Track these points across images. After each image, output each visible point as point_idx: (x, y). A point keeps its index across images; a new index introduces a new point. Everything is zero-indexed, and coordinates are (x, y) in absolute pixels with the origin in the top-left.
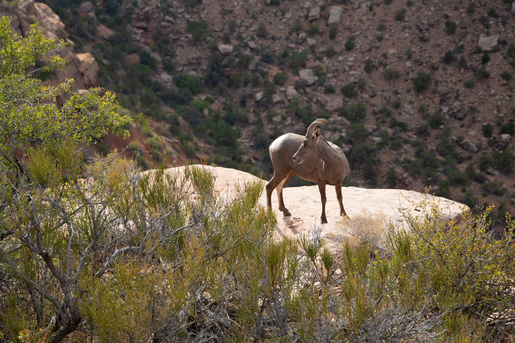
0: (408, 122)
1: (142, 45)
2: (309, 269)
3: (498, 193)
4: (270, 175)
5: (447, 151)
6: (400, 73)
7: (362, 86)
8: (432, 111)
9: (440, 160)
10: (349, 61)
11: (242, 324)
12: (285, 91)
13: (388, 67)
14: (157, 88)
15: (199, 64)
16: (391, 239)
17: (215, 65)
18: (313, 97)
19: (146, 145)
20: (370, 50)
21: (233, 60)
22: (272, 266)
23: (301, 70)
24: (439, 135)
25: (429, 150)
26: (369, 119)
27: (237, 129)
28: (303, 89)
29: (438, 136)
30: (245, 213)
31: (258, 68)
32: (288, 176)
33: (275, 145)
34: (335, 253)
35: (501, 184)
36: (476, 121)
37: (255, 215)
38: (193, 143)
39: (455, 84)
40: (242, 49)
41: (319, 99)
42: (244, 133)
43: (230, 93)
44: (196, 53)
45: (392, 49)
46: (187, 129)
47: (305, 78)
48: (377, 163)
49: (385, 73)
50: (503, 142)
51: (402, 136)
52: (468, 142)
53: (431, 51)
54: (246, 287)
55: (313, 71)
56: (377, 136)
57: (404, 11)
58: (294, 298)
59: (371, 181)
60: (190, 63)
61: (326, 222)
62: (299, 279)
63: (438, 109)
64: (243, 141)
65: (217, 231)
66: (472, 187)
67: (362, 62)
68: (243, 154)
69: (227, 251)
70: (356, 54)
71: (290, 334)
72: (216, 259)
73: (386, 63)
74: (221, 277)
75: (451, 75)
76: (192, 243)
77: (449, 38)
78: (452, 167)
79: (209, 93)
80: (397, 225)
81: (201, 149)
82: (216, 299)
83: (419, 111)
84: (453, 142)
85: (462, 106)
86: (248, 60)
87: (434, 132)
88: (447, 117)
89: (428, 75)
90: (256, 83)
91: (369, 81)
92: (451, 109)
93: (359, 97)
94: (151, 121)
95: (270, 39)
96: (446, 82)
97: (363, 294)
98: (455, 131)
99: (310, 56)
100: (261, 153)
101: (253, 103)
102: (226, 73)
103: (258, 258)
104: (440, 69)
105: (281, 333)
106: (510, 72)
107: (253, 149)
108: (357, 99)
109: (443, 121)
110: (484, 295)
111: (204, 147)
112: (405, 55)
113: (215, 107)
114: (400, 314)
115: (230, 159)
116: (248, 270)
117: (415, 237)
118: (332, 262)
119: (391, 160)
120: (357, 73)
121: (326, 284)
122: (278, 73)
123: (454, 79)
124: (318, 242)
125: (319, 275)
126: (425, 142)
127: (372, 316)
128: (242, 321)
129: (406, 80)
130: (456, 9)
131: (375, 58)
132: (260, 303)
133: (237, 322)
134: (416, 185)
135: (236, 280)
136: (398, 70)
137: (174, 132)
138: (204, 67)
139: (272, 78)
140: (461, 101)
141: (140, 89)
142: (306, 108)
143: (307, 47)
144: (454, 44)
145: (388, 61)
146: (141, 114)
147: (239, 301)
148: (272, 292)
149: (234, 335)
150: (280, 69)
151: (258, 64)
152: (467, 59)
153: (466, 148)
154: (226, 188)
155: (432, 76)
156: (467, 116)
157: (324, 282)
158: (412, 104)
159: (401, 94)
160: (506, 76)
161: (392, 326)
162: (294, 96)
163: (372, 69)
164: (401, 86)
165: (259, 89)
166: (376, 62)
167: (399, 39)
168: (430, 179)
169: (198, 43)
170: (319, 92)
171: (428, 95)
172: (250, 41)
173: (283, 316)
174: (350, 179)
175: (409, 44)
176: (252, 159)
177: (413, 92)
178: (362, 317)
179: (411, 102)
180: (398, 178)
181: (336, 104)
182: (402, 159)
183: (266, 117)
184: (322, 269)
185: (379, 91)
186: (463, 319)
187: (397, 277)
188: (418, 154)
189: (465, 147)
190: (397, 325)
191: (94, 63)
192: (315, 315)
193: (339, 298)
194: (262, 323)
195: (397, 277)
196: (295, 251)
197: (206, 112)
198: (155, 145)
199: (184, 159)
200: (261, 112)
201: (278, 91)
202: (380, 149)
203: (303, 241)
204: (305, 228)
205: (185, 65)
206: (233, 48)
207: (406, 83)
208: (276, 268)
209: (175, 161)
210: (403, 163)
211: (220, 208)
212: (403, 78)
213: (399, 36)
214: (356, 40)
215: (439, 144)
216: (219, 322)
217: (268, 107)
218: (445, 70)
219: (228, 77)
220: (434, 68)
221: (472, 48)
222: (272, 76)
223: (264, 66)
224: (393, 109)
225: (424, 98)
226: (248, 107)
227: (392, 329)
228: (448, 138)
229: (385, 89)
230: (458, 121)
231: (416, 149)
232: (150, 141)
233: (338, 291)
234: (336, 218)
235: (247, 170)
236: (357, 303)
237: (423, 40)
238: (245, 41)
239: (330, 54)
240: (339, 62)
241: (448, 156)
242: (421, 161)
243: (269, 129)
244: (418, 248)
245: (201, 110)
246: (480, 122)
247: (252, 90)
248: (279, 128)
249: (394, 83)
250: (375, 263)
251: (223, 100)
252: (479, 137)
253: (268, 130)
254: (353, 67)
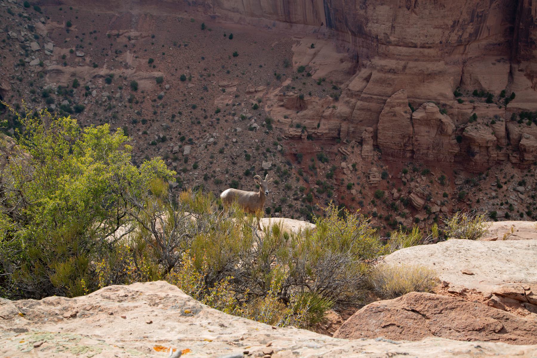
57: (223, 149)
130: (250, 148)
145: (216, 175)
220: (240, 178)
237: (234, 163)
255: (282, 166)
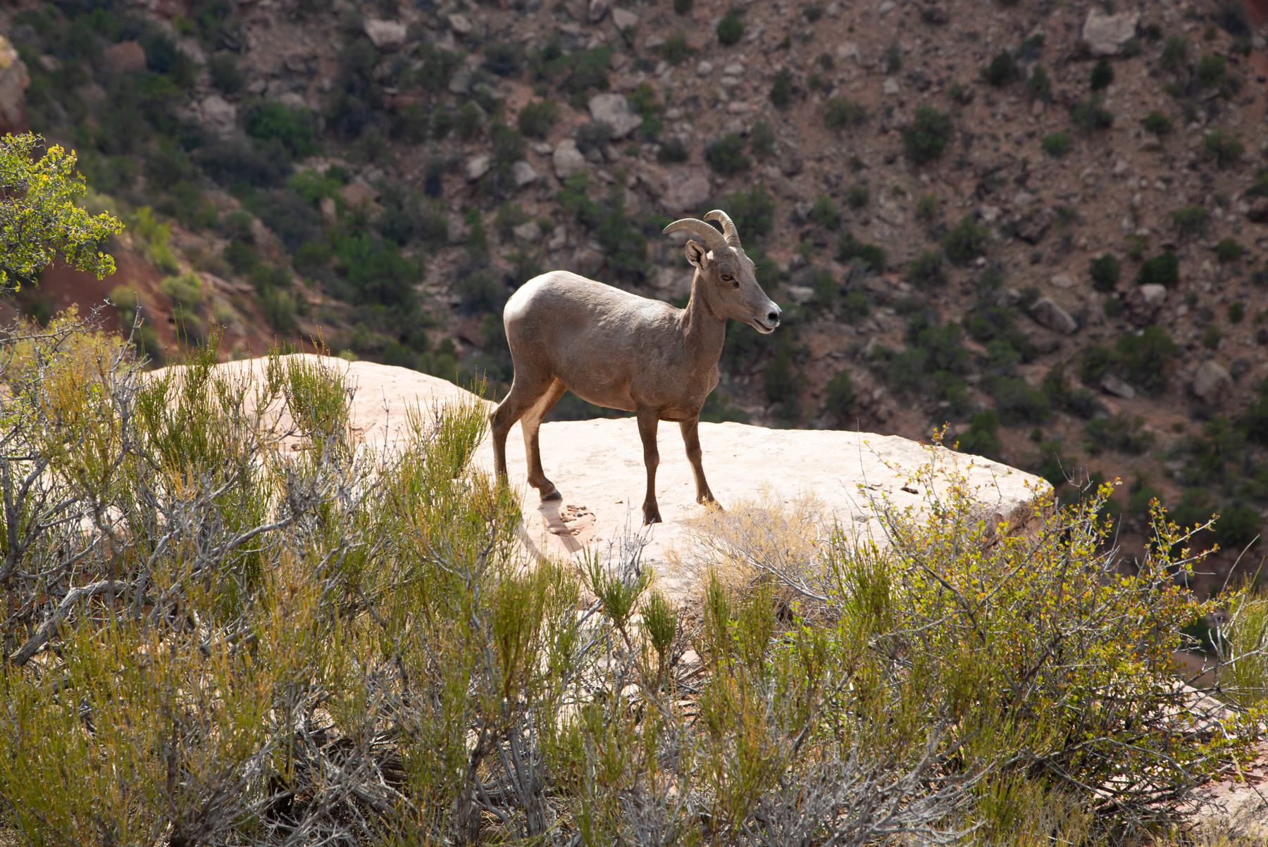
0: (888, 247)
1: (152, 17)
2: (608, 650)
3: (1131, 447)
4: (505, 386)
5: (993, 329)
6: (869, 112)
7: (762, 144)
8: (954, 217)
9: (973, 353)
10: (728, 75)
11: (421, 800)
12: (551, 154)
13: (835, 93)
14: (193, 137)
15: (311, 74)
16: (836, 570)
17: (355, 77)
18: (628, 171)
19: (158, 297)
20: (786, 45)
21: (407, 65)
22: (505, 638)
23: (594, 95)
24: (974, 283)
25: (944, 324)
26: (782, 235)
27: (415, 256)
28: (601, 149)
29: (969, 286)
30: (433, 492)
31: (477, 87)
32: (552, 388)
33: (517, 304)
34: (682, 605)
35: (1140, 422)
36: (1075, 247)
37: (460, 496)
38: (290, 294)
39: (1019, 143)
40: (432, 35)
41: (645, 177)
42: (433, 267)
43: (398, 155)
44: (304, 44)
45: (847, 44)
46: (275, 254)
47: (605, 119)
48: (800, 357)
49: (827, 110)
50: (1146, 305)
51: (871, 286)
52: (1049, 306)
53: (953, 51)
54: (432, 697)
55: (629, 100)
56: (801, 285)
58: (565, 728)
59: (785, 409)
60: (286, 72)
61: (658, 520)
62: (580, 677)
63: (969, 211)
64: (432, 290)
65: (354, 541)
66: (1061, 429)
67: (764, 79)
68: (429, 325)
69: (381, 595)
70: (747, 56)
71: (554, 829)
72: (351, 619)
73: (830, 81)
74: (364, 668)
75: (1007, 119)
76: (285, 572)
77: (1003, 15)
78: (1006, 374)
79: (339, 156)
80: (852, 531)
81: (315, 311)
82: (348, 731)
83: (918, 217)
84: (1010, 305)
85: (1036, 206)
86: (449, 65)
87: (959, 276)
88: (995, 234)
89: (946, 118)
90: (469, 131)
91: (783, 132)
92: (1006, 212)
93: (753, 175)
94: (175, 229)
95: (510, 7)
96: (994, 138)
97: (758, 722)
98: (1017, 274)
99: (620, 59)
100: (481, 325)
101: (460, 186)
102: (387, 102)
103: (468, 617)
104: (978, 101)
105: (528, 825)
106: (1167, 113)
107: (458, 314)
108: (747, 180)
109: (983, 244)
110: (1089, 728)
111: (321, 306)
112: (881, 60)
113: (355, 193)
114: (857, 776)
115: (393, 340)
116: (439, 648)
117: (903, 565)
118: (672, 629)
119: (838, 351)
120: (751, 108)
121: (654, 693)
122: (531, 104)
123: (1017, 131)
124: (634, 576)
125: (637, 666)
126: (933, 301)
127: (780, 782)
128: (419, 792)
129: (884, 131)
131: (799, 68)
132: (471, 741)
133: (407, 795)
134: (906, 422)
135: (405, 678)
136: (862, 103)
137: (239, 259)
138: (327, 83)
139: (515, 118)
140: (1033, 192)
141: (145, 140)
142: (608, 203)
143: (613, 33)
144: (1017, 34)
146: (147, 210)
147: (412, 735)
148: (504, 713)
149: (394, 829)
150: (538, 94)
151: (475, 79)
152: (1050, 75)
153: (1044, 320)
154: (382, 421)
155: (955, 121)
156: (1049, 232)
157: (650, 685)
158: (900, 197)
159: (868, 168)
160: (1157, 125)
161: (836, 811)
162: (574, 169)
163: (792, 97)
164: (870, 147)
165: (476, 147)
166: (801, 79)
167: (865, 15)
168: (944, 404)
169: (310, 16)
170: (645, 157)
171: (943, 172)
172: (455, 11)
173: (535, 780)
174: (725, 401)
175: (894, 30)
176: (455, 342)
177: (901, 163)
178: (752, 783)
179: (897, 192)
180: (858, 400)
181: (690, 192)
182: (869, 349)
183: (496, 224)
184: (644, 648)
185: (808, 159)
186: (1031, 793)
187: (850, 674)
188: (913, 336)
189: (1042, 317)
190: (847, 806)
191: (15, 64)
192: (624, 777)
193: (690, 730)
194: (474, 796)
195: (850, 674)
196: (570, 598)
197: (329, 207)
198: (186, 298)
199: (265, 339)
200: (482, 212)
201: (529, 154)
202: (808, 319)
203: (594, 572)
204: (599, 535)
205: (274, 76)
206: (408, 32)
207: (883, 139)
208: (518, 646)
209: (240, 344)
210: (872, 358)
211: (364, 475)
212: (875, 125)
213: (866, 8)
214: (748, 17)
215: (970, 308)
216: (354, 794)
217: (502, 198)
218: (990, 103)
219: (392, 111)
220: (961, 99)
221: (1064, 46)
222: (513, 111)
223: (493, 85)
224: (846, 208)
225: (933, 181)
226: (445, 196)
227: (834, 818)
228: (995, 293)
229: (827, 153)
230: (1024, 246)
231: (910, 320)
232: (170, 286)
233: (688, 711)
234: (686, 509)
235: (441, 373)
236: (740, 745)
238: (440, 13)
239: (676, 53)
240: (702, 76)
241: (996, 343)
242: (921, 354)
243: (505, 257)
244: (911, 595)
245: (317, 203)
246: (1084, 249)
247: (458, 150)
248: (531, 255)
249: (851, 137)
250: (792, 635)
251: (376, 175)
252: (1083, 290)
253: (501, 260)
254: (738, 92)
255: (1196, 37)
